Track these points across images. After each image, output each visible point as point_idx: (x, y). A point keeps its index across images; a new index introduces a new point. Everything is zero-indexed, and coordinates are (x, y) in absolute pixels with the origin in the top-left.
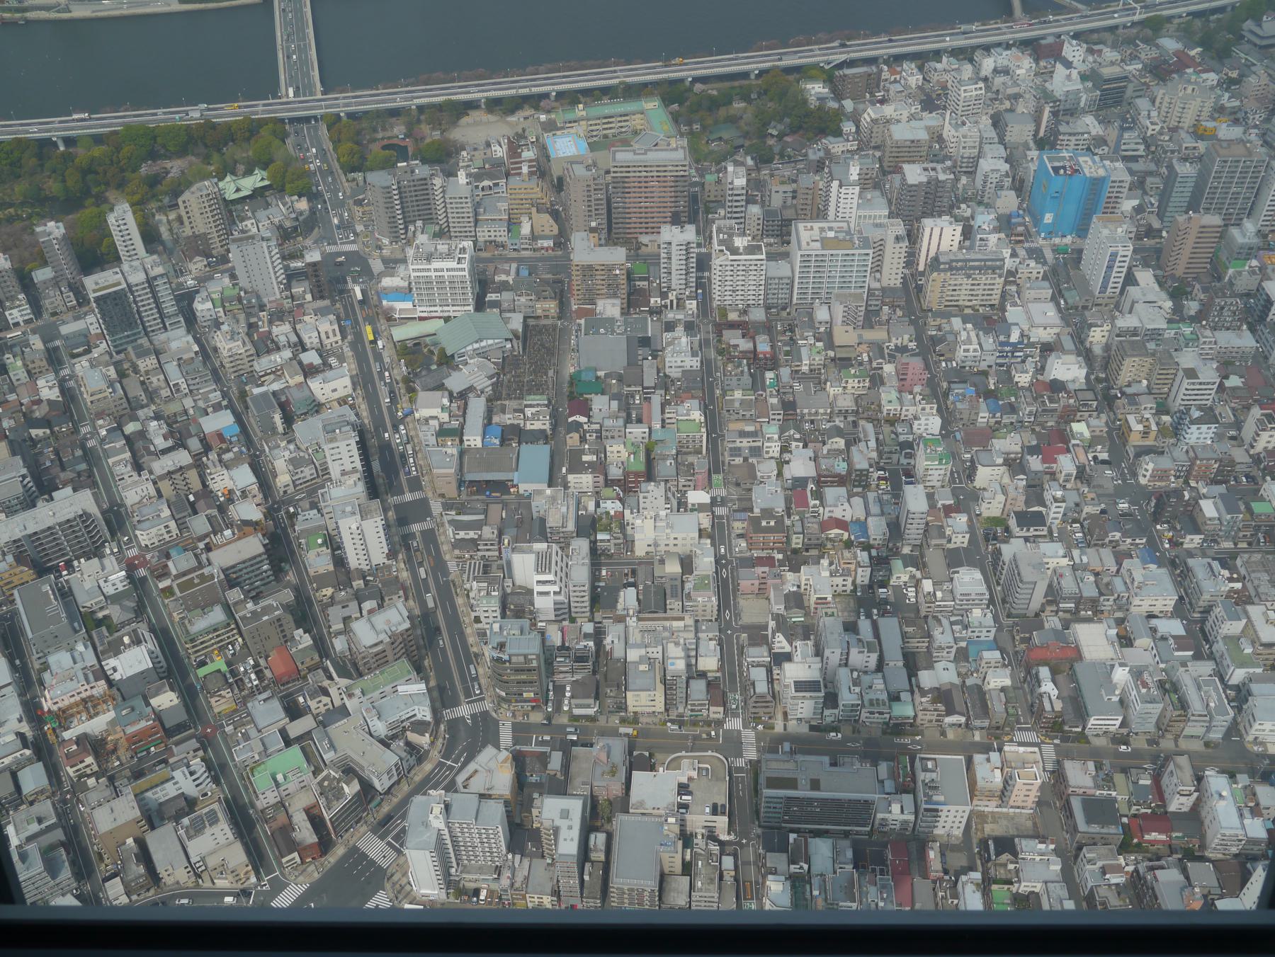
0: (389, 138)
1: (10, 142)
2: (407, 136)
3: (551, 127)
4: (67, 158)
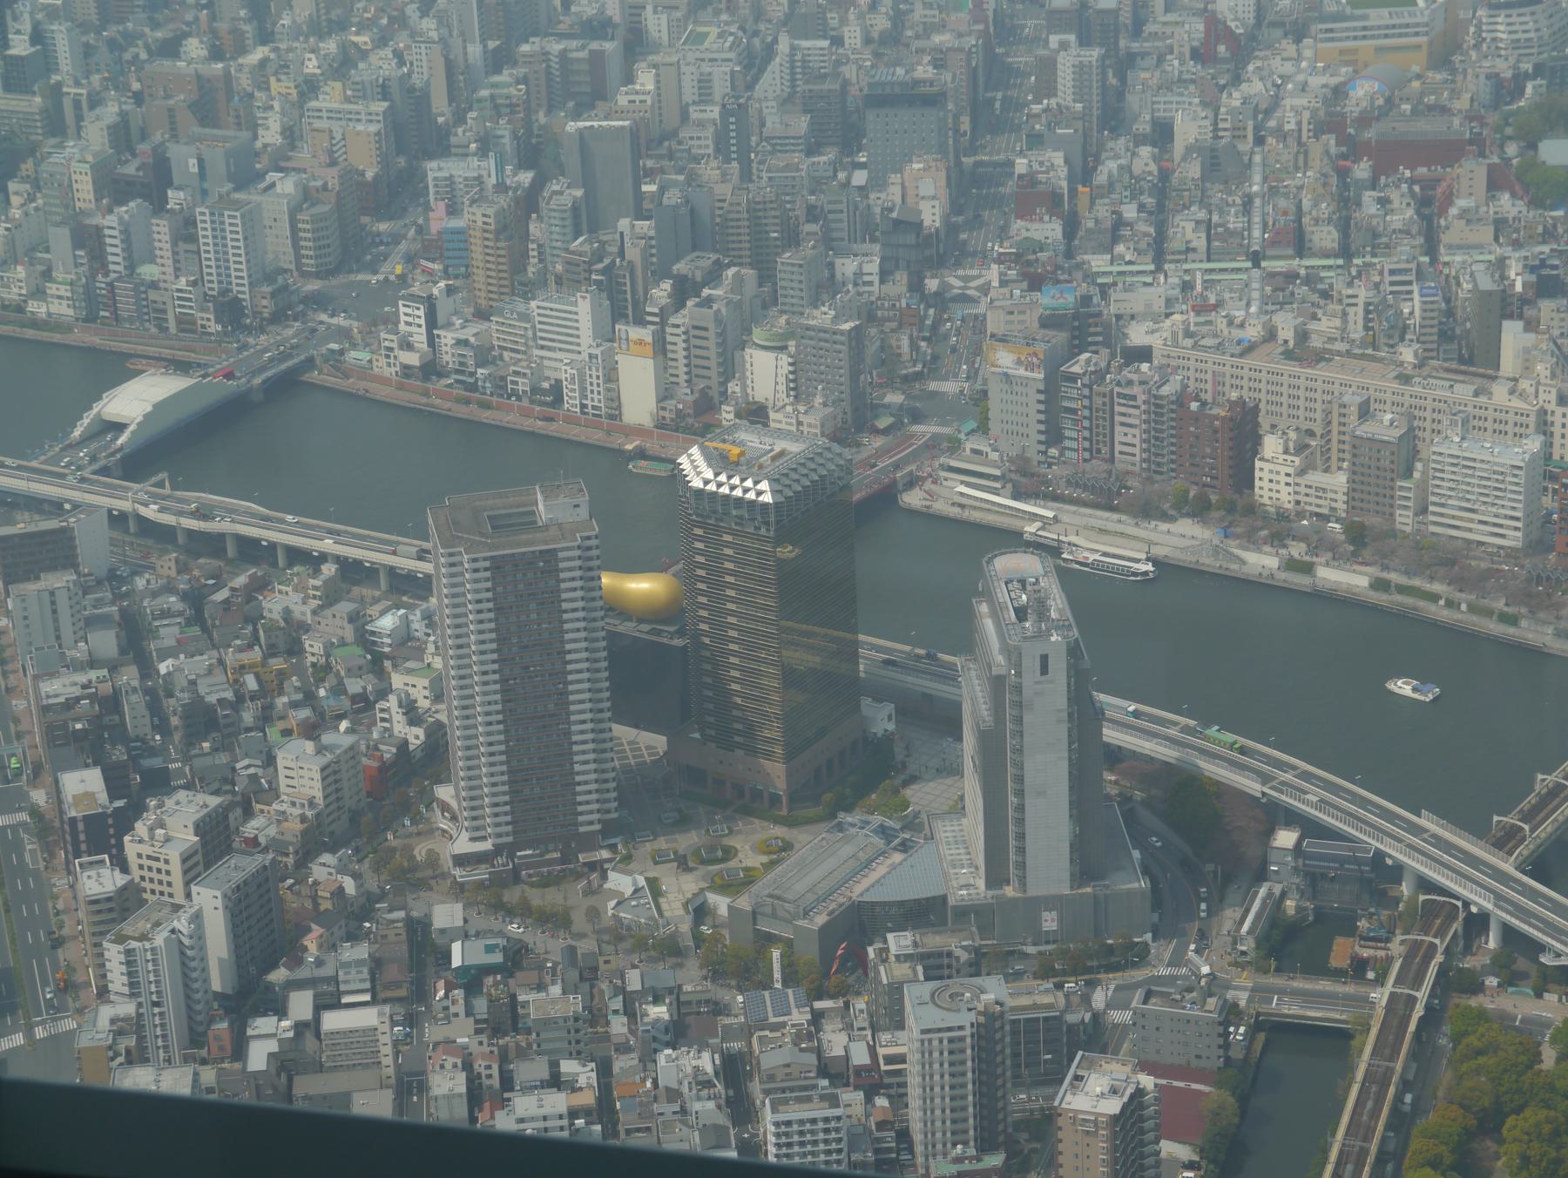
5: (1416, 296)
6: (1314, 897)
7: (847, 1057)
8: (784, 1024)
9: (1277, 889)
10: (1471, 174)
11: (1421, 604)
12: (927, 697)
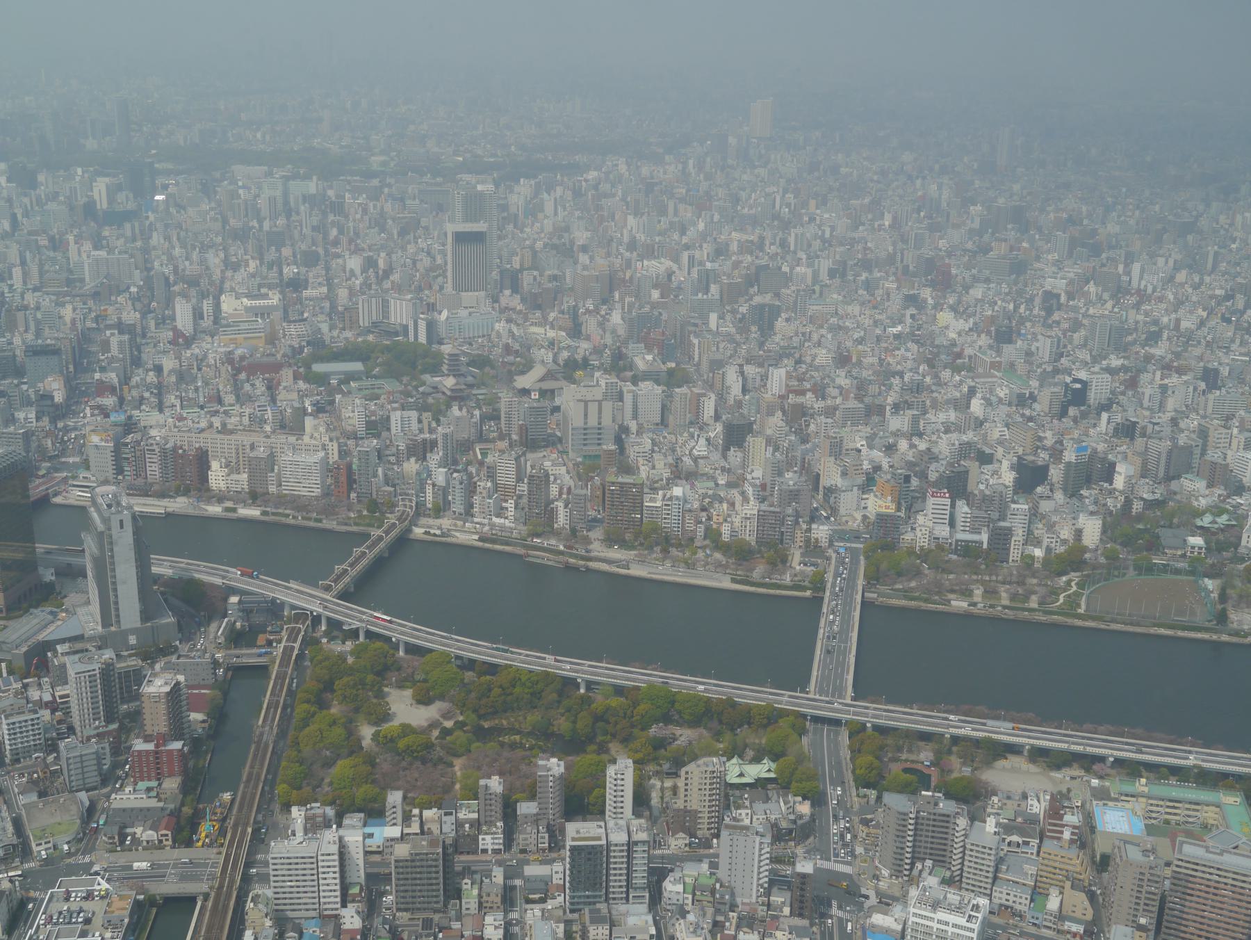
0: (913, 762)
1: (538, 674)
2: (933, 764)
3: (1102, 795)
4: (586, 701)
5: (269, 411)
6: (248, 621)
7: (41, 699)
8: (9, 690)
9: (233, 619)
10: (287, 375)
11: (283, 519)
12: (69, 565)
